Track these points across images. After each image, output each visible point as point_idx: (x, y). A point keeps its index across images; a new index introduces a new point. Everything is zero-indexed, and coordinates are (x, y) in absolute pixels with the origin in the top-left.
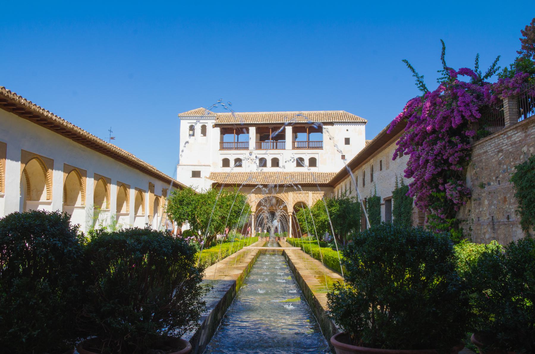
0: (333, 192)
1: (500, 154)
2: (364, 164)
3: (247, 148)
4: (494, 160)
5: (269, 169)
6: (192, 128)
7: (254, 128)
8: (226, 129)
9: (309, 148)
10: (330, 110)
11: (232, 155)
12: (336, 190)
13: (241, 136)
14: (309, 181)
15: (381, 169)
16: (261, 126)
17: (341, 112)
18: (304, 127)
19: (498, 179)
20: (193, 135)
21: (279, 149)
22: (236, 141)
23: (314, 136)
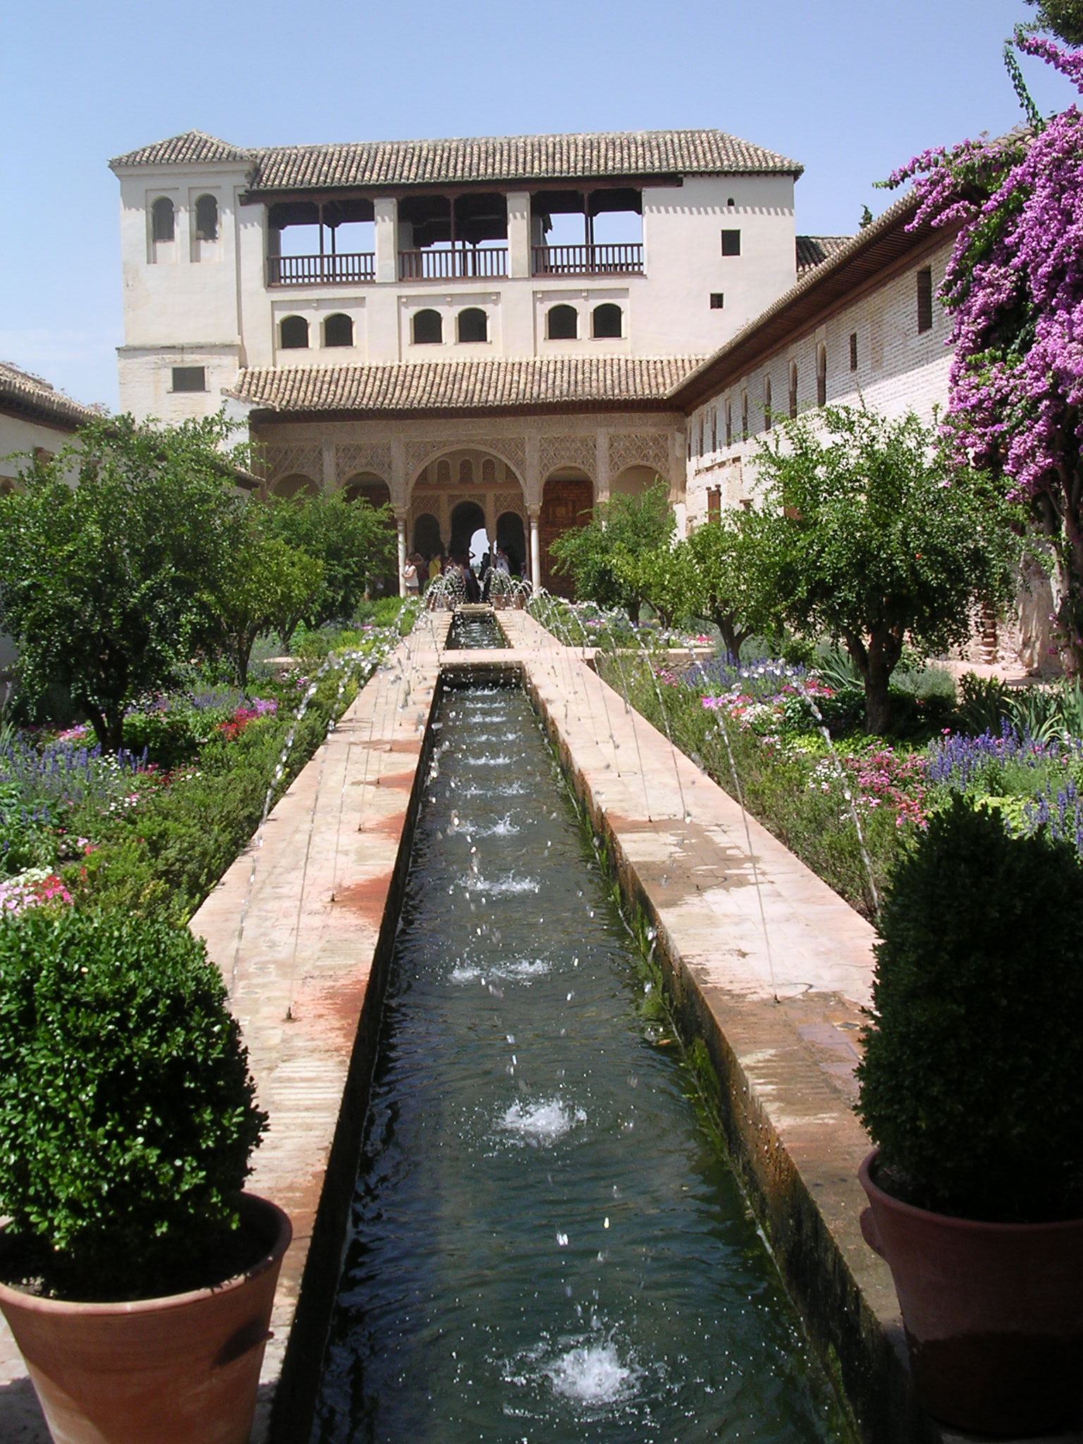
0: (683, 430)
9: (593, 269)
12: (693, 420)
13: (344, 229)
15: (854, 366)
16: (418, 193)
18: (575, 192)
23: (612, 226)
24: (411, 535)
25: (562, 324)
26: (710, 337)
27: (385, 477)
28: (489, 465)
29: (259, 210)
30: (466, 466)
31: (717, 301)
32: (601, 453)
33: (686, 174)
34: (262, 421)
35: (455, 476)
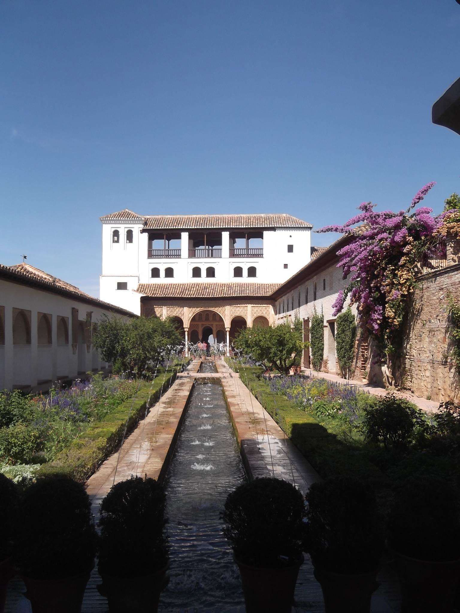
1: (441, 293)
2: (307, 281)
3: (179, 256)
4: (435, 298)
5: (204, 279)
6: (116, 233)
7: (187, 233)
8: (154, 235)
10: (272, 213)
11: (162, 264)
12: (277, 303)
13: (172, 241)
14: (248, 293)
15: (324, 289)
17: (284, 215)
18: (243, 232)
19: (438, 318)
20: (118, 241)
21: (215, 257)
22: (167, 248)
23: (254, 242)
24: (190, 336)
25: (238, 272)
26: (283, 277)
27: (182, 318)
28: (215, 315)
29: (146, 235)
30: (207, 315)
31: (286, 266)
32: (249, 313)
33: (277, 227)
34: (143, 299)
35: (204, 319)
